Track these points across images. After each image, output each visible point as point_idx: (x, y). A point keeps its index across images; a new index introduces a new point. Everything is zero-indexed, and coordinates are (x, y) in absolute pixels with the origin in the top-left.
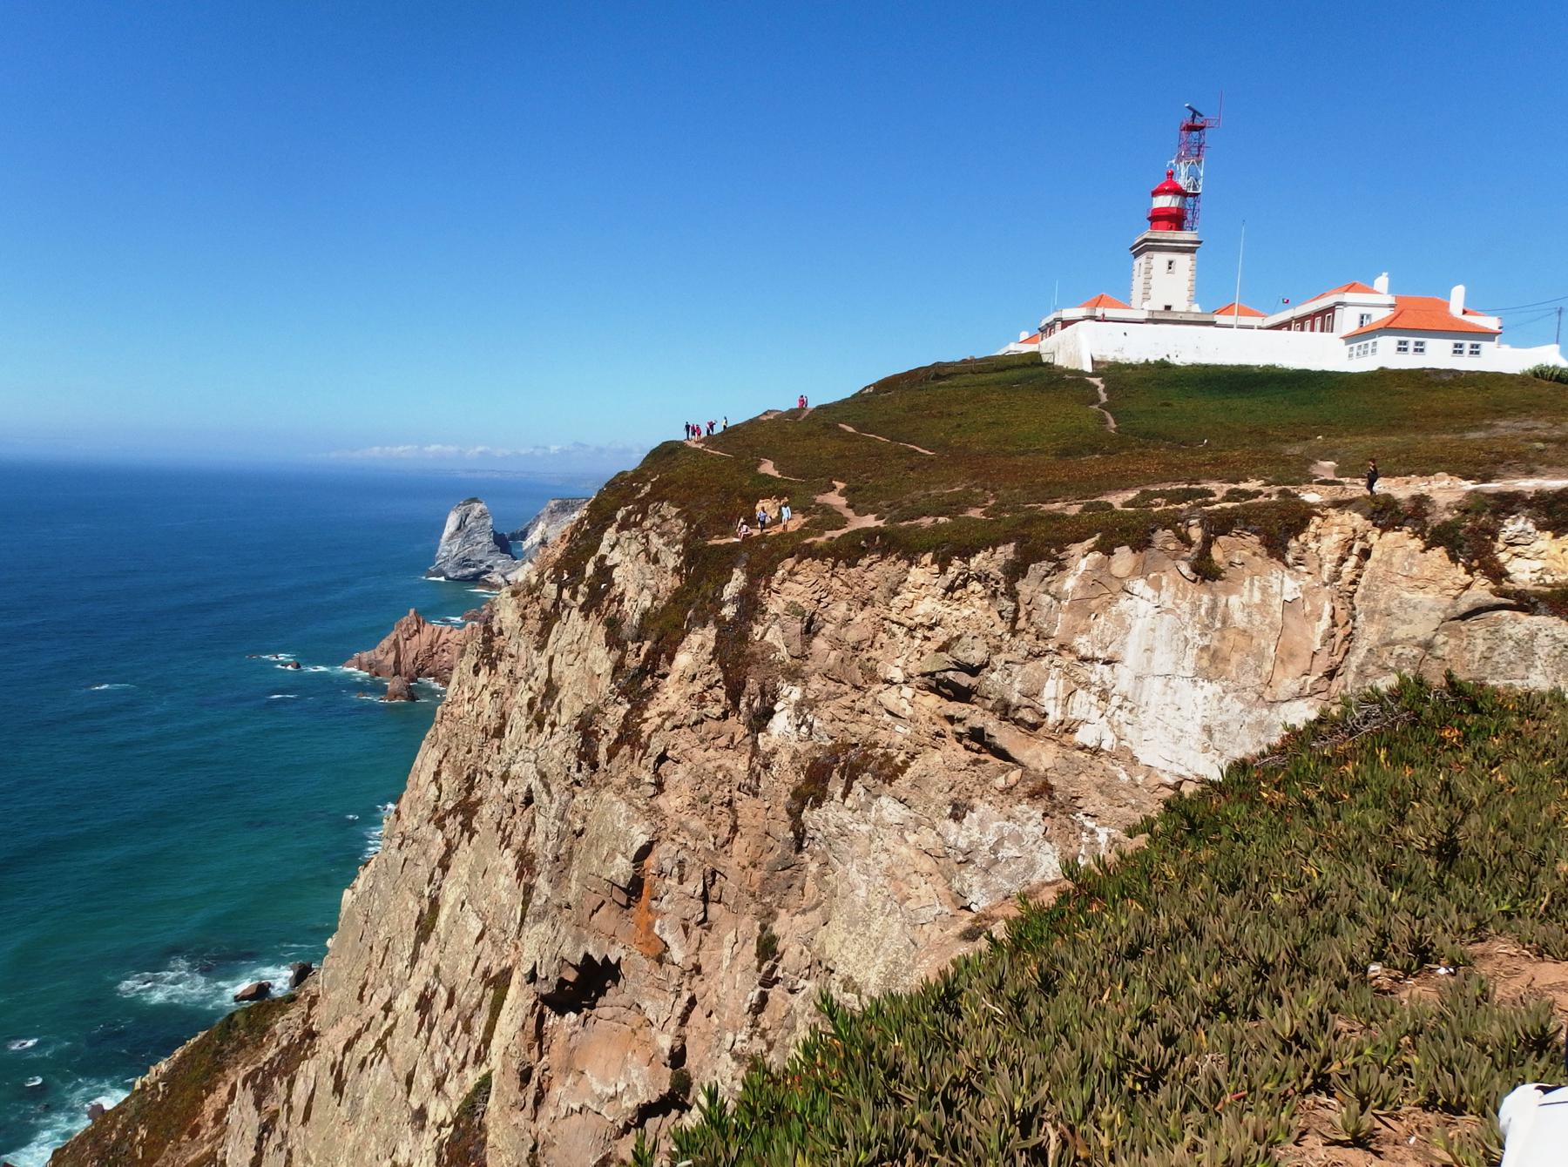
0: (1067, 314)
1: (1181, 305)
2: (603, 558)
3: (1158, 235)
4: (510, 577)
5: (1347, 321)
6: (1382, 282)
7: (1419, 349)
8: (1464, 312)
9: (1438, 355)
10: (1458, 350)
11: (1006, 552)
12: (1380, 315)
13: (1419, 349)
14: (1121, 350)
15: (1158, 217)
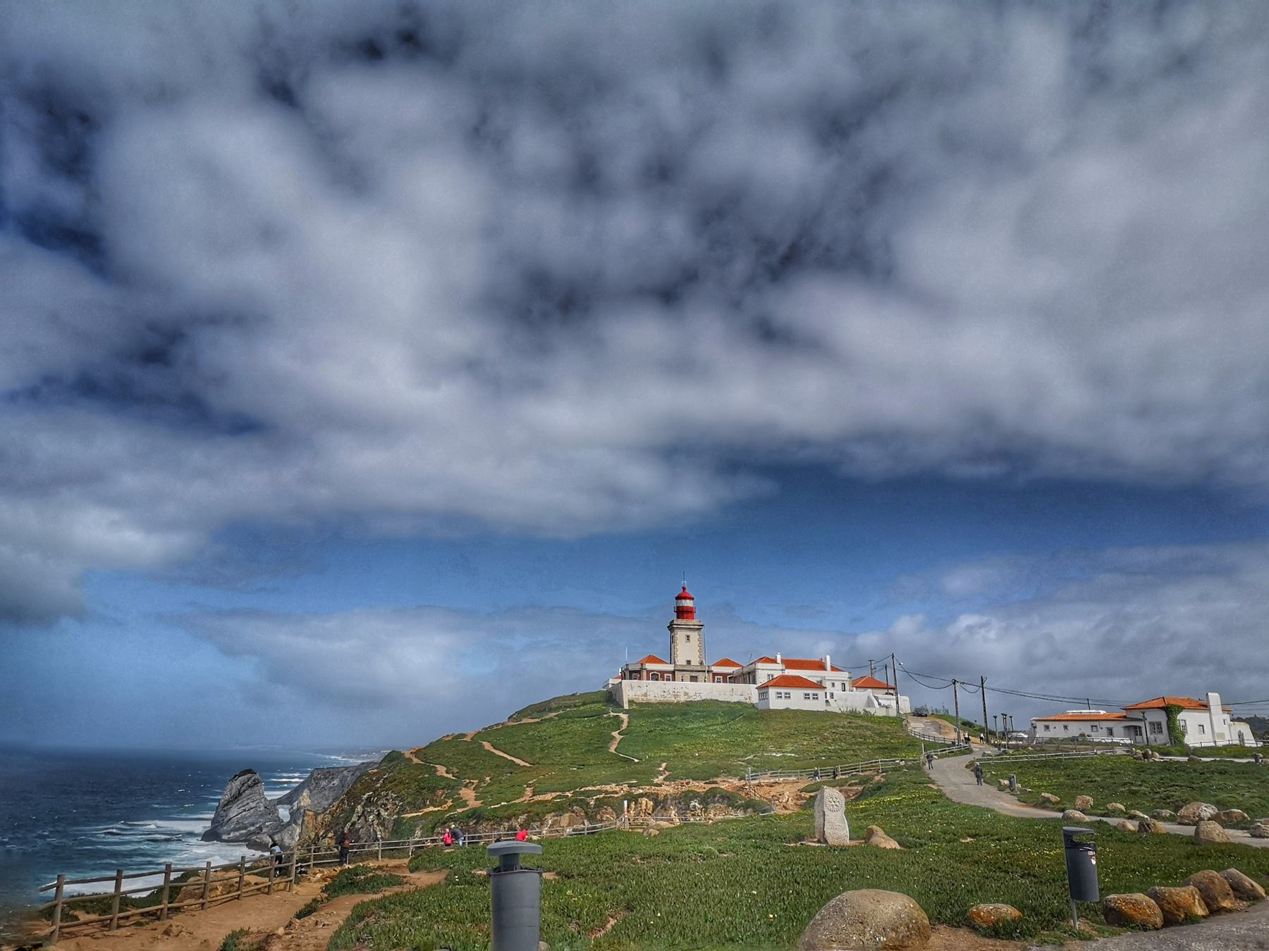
0: (631, 668)
1: (695, 662)
2: (354, 824)
3: (680, 621)
4: (276, 838)
5: (762, 678)
6: (779, 658)
7: (788, 696)
8: (833, 669)
9: (797, 700)
10: (807, 696)
11: (522, 818)
12: (777, 674)
13: (788, 696)
14: (645, 695)
15: (682, 612)
